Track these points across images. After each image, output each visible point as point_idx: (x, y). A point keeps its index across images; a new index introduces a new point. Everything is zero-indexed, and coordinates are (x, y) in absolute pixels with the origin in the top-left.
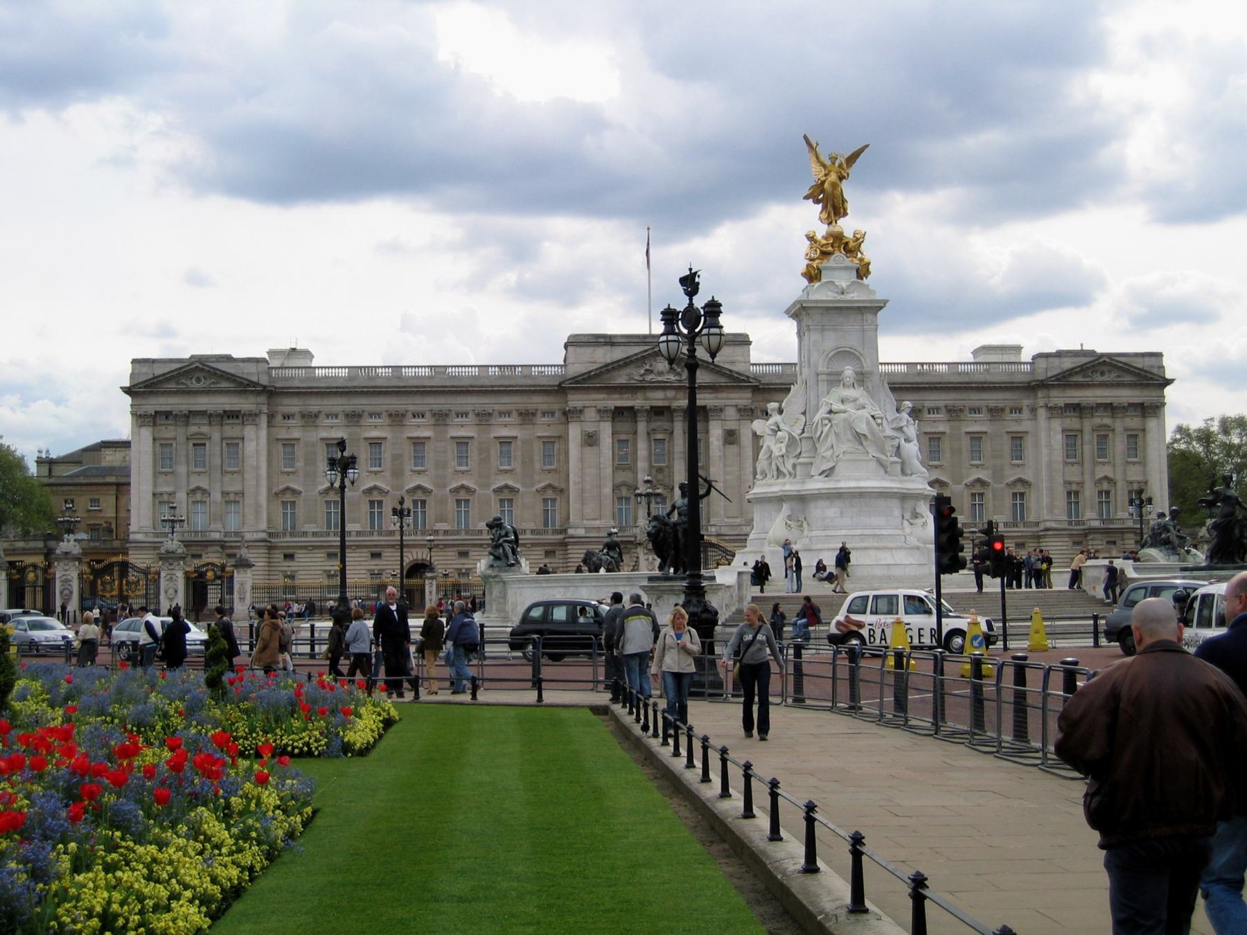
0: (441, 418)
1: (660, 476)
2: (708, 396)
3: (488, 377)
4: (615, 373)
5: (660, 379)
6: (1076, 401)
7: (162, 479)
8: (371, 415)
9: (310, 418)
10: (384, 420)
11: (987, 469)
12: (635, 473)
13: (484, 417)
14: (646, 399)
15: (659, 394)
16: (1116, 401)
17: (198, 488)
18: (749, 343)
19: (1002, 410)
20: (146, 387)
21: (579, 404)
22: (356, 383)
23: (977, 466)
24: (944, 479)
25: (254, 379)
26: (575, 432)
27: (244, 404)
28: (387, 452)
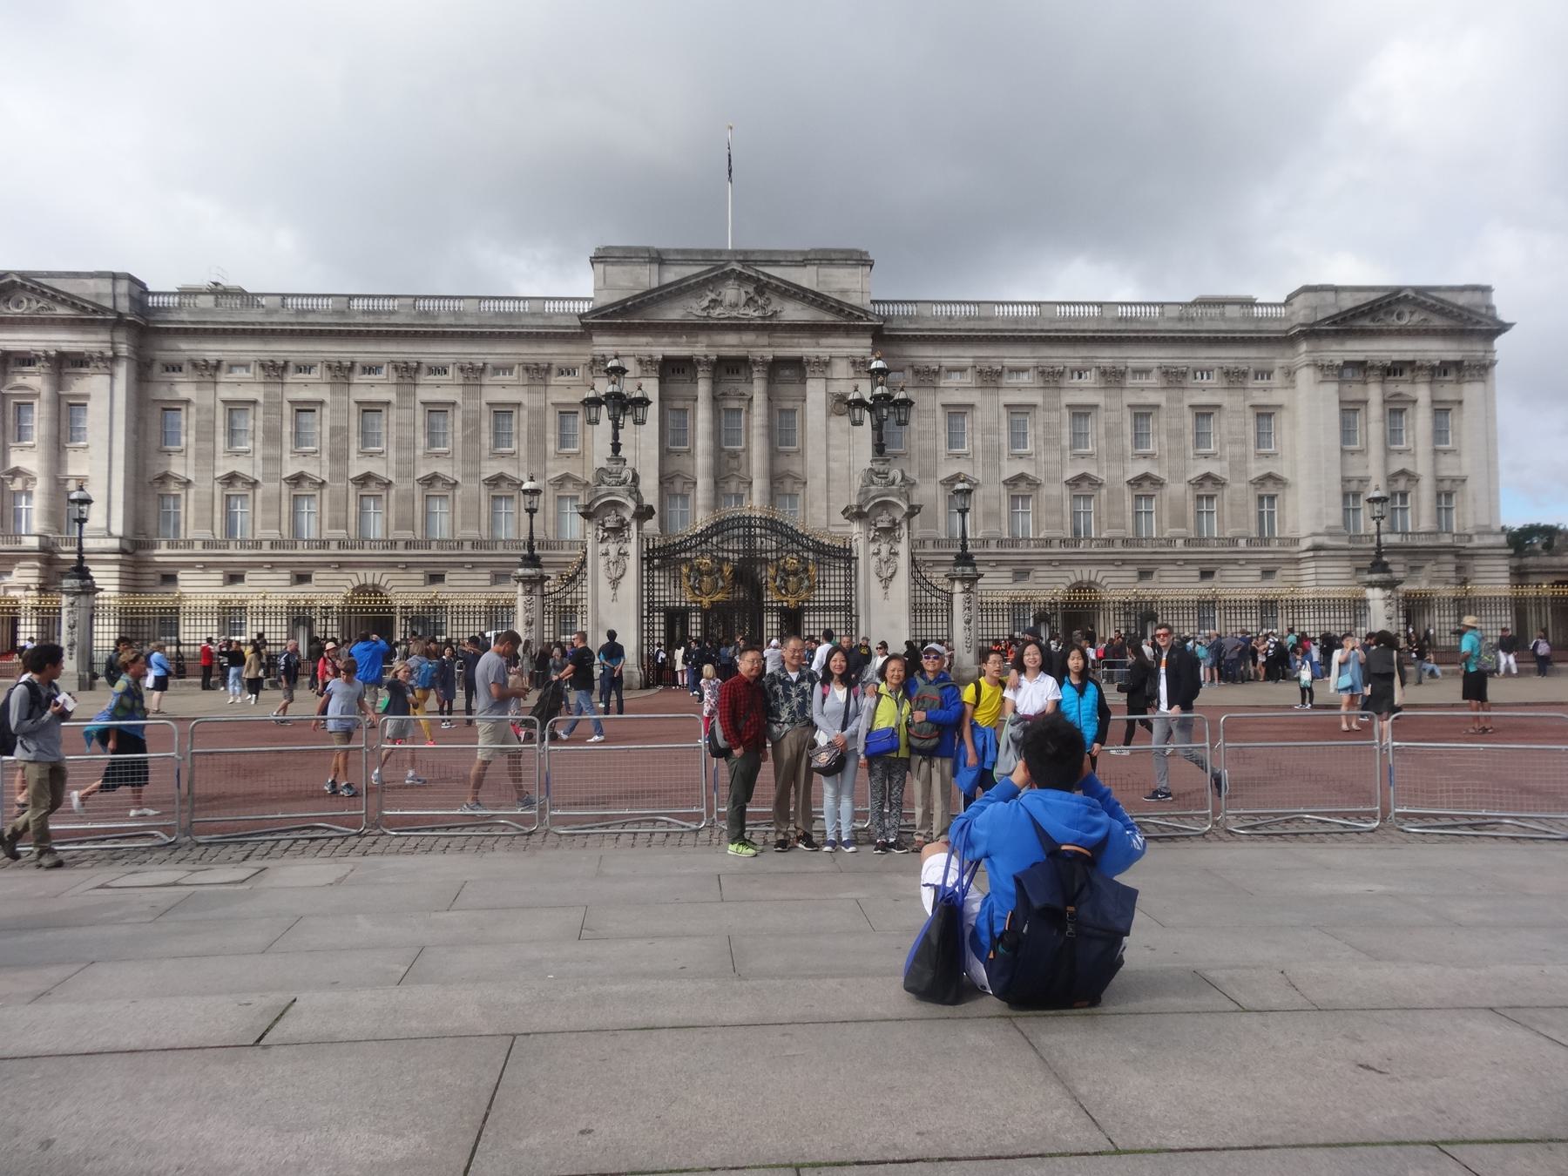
0: (408, 373)
1: (733, 463)
3: (478, 314)
5: (734, 314)
6: (1360, 357)
8: (300, 369)
11: (1220, 459)
12: (694, 457)
13: (473, 374)
15: (731, 338)
16: (1417, 357)
18: (869, 264)
19: (1245, 374)
22: (275, 319)
24: (1155, 472)
25: (108, 304)
28: (322, 426)
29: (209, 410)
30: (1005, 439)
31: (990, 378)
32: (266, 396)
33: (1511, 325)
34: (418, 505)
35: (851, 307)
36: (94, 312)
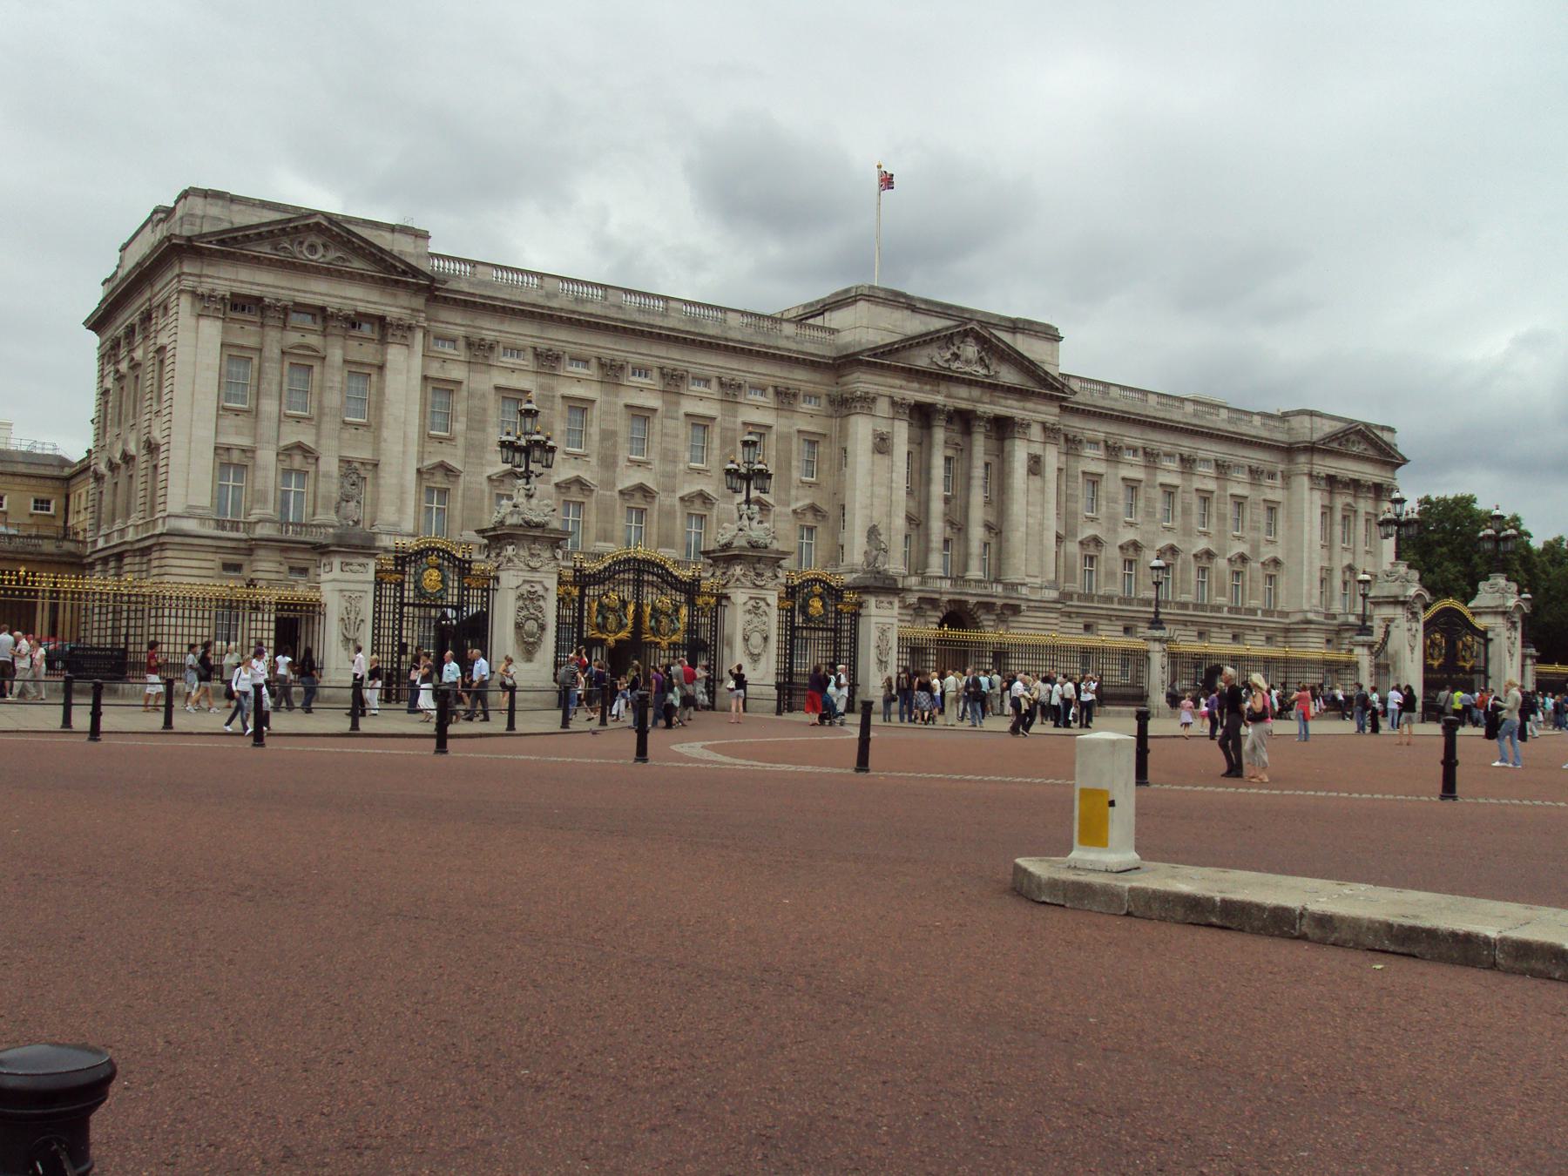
0: (673, 380)
2: (1015, 403)
4: (915, 352)
5: (967, 369)
6: (1332, 472)
7: (229, 421)
8: (571, 359)
9: (480, 351)
10: (592, 372)
13: (731, 390)
14: (949, 396)
15: (963, 392)
17: (299, 446)
20: (222, 242)
21: (872, 389)
22: (554, 304)
23: (1239, 538)
26: (862, 429)
27: (393, 306)
29: (483, 396)
30: (1121, 508)
31: (1113, 452)
32: (541, 387)
33: (1405, 461)
34: (678, 521)
35: (1054, 378)
36: (404, 273)
